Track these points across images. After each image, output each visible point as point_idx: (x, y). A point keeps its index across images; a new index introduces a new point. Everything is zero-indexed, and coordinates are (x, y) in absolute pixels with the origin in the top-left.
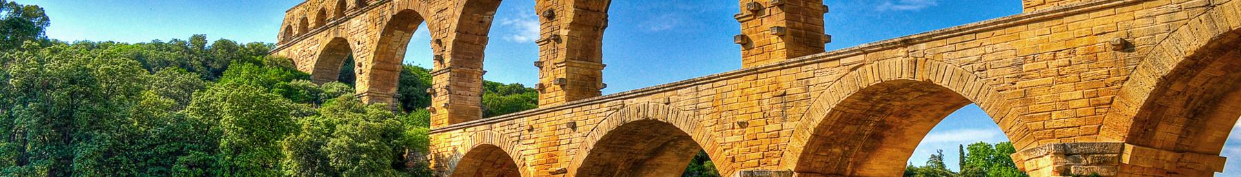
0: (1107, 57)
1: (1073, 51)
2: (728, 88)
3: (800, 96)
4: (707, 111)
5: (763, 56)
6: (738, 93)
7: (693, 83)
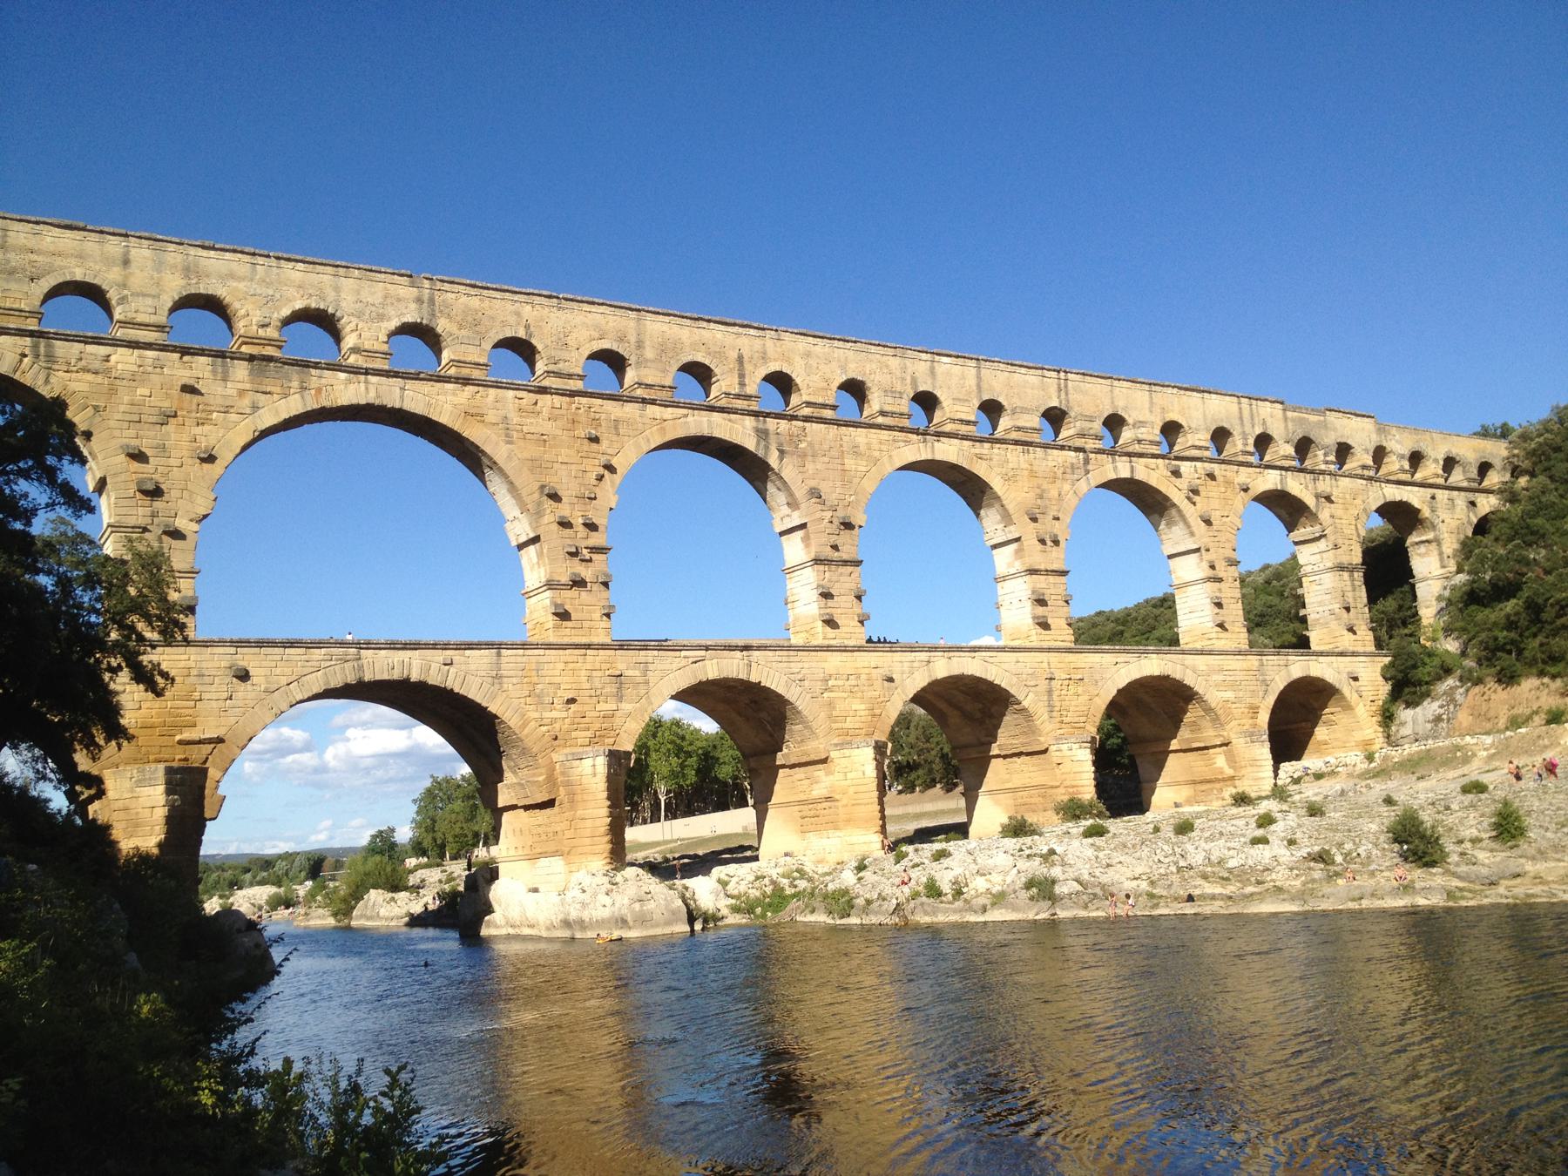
0: (878, 684)
1: (858, 677)
2: (544, 659)
3: (641, 679)
4: (514, 680)
5: (580, 632)
6: (562, 666)
7: (498, 646)
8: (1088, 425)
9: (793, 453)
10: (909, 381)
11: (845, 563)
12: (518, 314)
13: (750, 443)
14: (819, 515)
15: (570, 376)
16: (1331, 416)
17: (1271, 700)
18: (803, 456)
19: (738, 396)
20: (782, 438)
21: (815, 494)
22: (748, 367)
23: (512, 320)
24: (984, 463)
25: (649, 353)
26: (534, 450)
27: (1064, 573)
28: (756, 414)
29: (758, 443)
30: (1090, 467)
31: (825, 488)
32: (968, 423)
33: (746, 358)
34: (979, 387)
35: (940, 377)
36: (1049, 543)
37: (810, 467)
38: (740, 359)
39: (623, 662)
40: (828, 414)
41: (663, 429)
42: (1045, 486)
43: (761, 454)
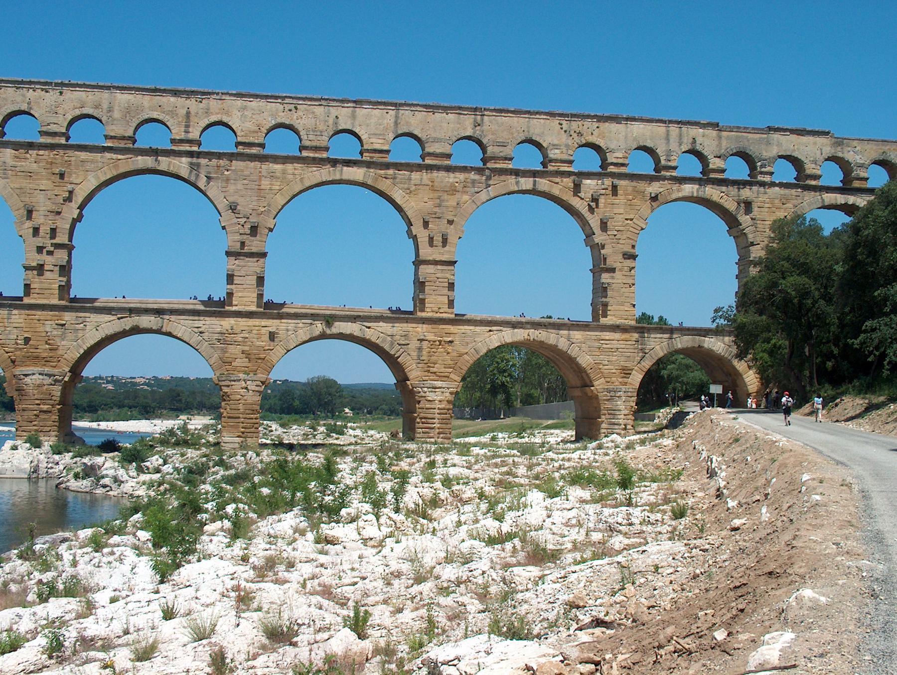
0: (266, 337)
1: (250, 332)
8: (501, 149)
9: (218, 178)
10: (331, 121)
11: (251, 255)
12: (23, 96)
13: (184, 173)
14: (236, 220)
15: (54, 134)
16: (776, 136)
17: (647, 364)
18: (228, 180)
19: (181, 141)
20: (210, 169)
21: (233, 208)
22: (193, 119)
23: (19, 99)
24: (388, 182)
25: (117, 114)
26: (24, 183)
27: (453, 263)
28: (191, 154)
29: (191, 172)
30: (491, 182)
31: (240, 201)
32: (381, 151)
33: (193, 113)
34: (396, 123)
35: (360, 119)
36: (438, 239)
37: (231, 188)
38: (188, 114)
39: (68, 317)
40: (254, 151)
41: (116, 167)
43: (193, 179)
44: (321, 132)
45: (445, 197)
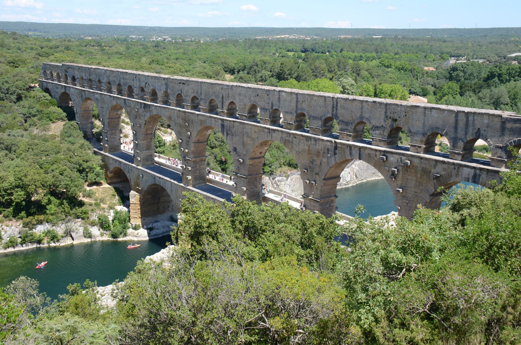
22: (224, 100)
30: (337, 151)
34: (297, 106)
35: (282, 102)
38: (223, 96)
42: (315, 158)
44: (266, 110)
45: (315, 158)
